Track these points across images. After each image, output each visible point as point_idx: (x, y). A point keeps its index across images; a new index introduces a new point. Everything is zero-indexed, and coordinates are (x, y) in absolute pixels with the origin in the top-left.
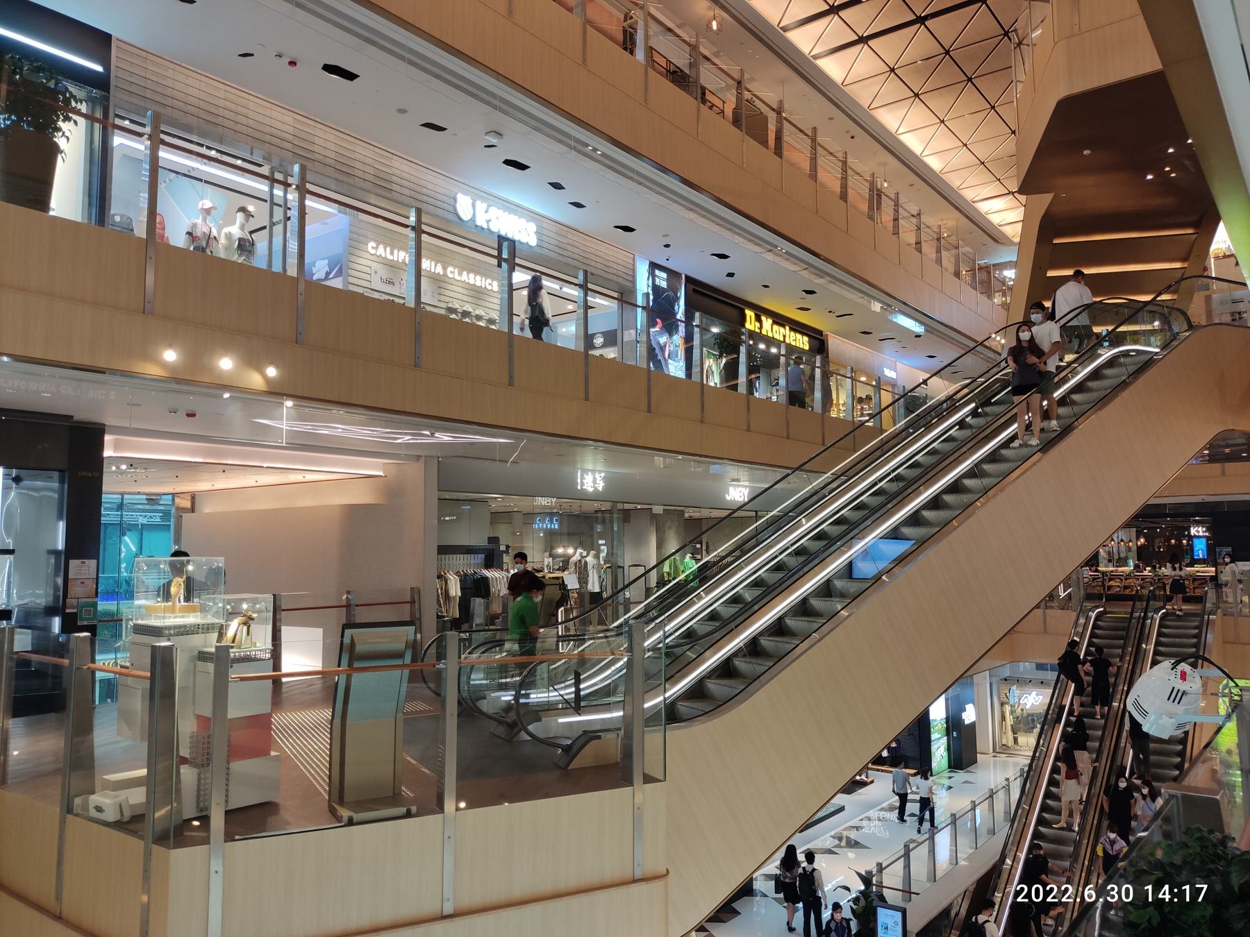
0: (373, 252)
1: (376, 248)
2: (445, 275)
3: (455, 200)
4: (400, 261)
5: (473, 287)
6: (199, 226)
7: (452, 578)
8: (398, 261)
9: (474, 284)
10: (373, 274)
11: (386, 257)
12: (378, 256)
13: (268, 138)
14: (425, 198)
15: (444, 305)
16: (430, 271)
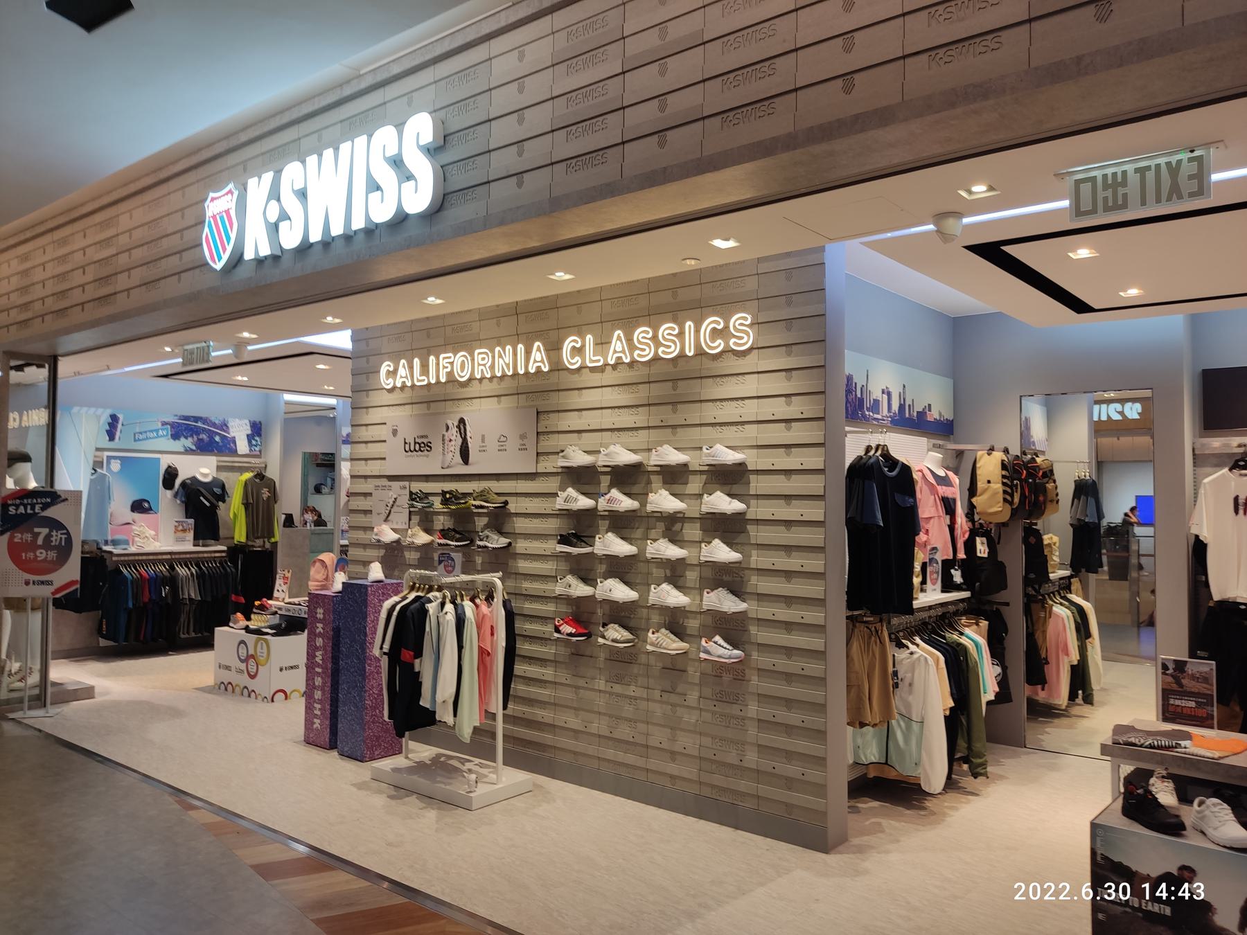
2: (558, 367)
4: (443, 380)
5: (655, 369)
8: (438, 382)
9: (656, 359)
15: (548, 465)
16: (515, 374)
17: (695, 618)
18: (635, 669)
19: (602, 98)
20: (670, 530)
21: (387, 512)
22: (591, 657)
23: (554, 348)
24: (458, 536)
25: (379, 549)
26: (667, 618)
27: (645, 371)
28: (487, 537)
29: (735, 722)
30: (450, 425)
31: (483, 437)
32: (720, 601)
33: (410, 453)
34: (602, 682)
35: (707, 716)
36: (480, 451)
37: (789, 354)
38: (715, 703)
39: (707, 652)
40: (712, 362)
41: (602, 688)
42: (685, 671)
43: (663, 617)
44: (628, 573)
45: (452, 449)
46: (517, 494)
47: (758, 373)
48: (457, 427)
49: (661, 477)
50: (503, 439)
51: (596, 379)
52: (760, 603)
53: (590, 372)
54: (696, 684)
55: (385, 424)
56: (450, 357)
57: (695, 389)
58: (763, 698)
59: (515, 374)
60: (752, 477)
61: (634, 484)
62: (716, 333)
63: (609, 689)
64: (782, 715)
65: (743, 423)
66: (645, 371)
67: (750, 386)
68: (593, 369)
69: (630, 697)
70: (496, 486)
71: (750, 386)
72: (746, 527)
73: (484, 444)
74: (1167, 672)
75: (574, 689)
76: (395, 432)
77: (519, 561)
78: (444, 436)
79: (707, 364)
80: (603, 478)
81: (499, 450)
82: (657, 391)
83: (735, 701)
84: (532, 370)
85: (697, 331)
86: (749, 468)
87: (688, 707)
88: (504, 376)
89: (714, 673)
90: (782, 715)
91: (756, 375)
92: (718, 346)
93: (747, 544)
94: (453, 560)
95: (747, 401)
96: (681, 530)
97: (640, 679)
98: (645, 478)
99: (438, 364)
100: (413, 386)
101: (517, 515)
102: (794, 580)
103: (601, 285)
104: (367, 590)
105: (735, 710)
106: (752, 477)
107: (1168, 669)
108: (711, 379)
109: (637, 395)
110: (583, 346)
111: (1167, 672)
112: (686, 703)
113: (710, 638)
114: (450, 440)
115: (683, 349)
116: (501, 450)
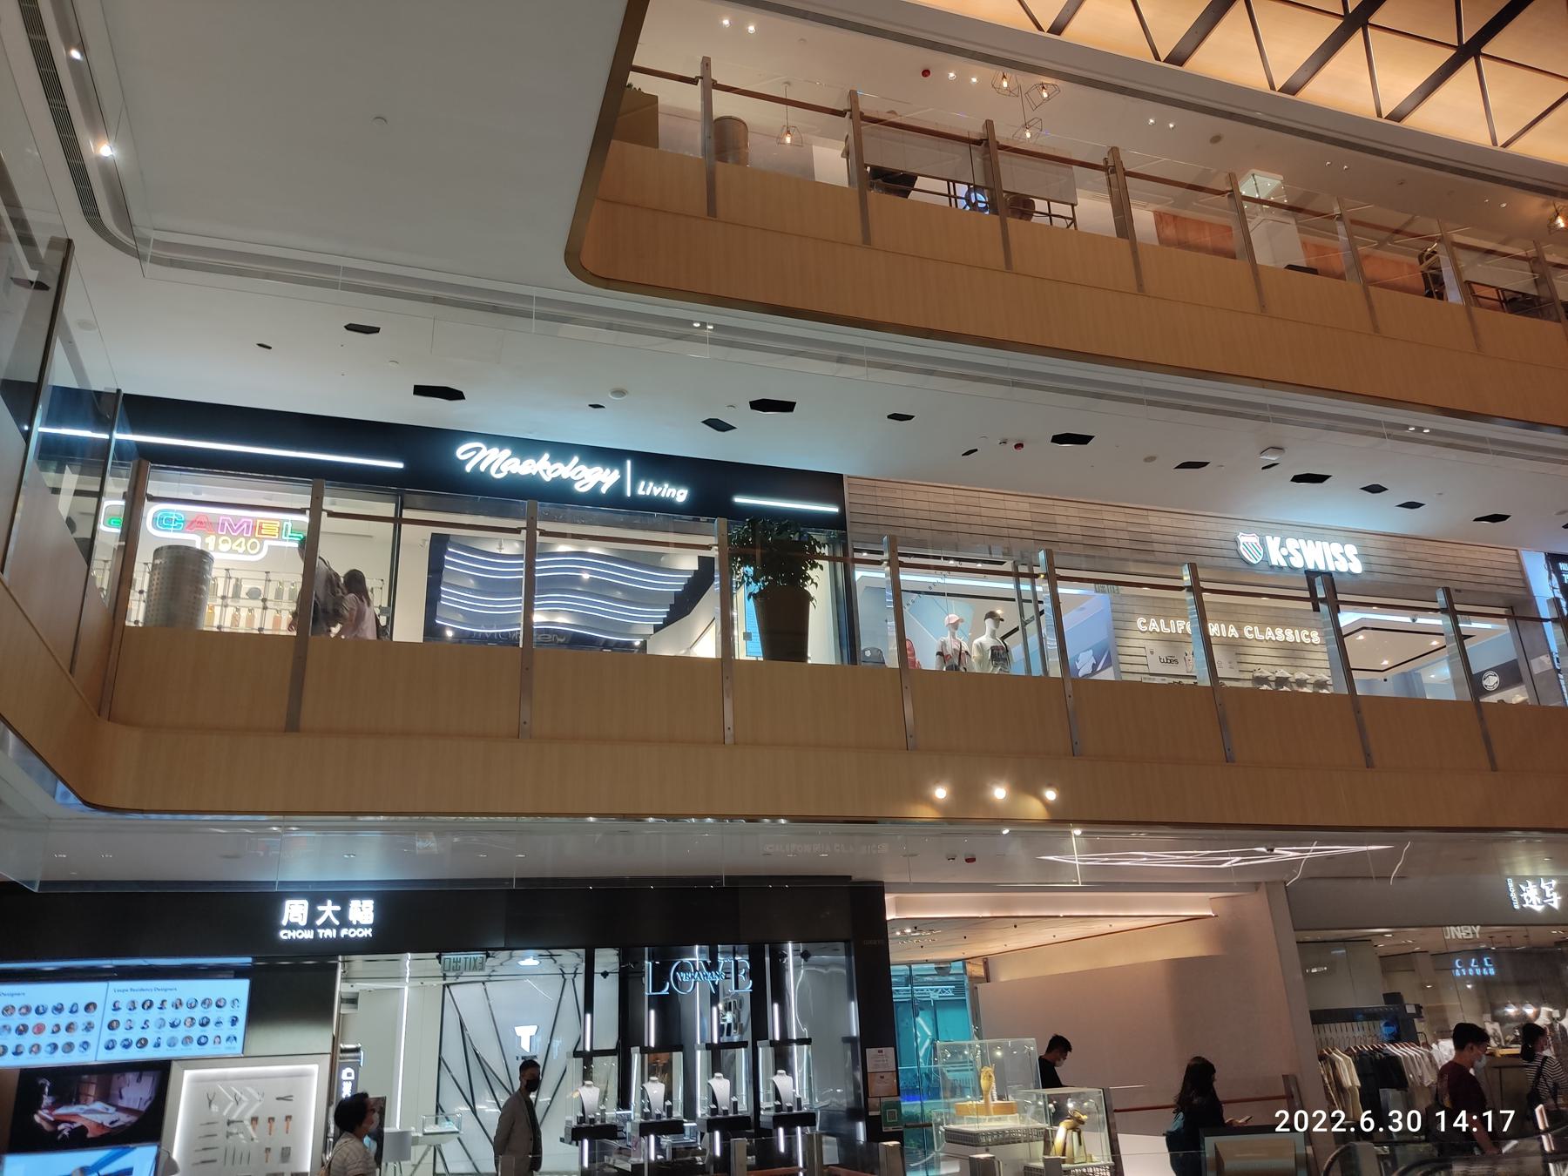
1: (1147, 624)
2: (1242, 637)
3: (1236, 542)
6: (949, 644)
7: (1339, 1058)
8: (1177, 633)
9: (1285, 641)
10: (1149, 655)
11: (1161, 632)
12: (1151, 632)
13: (1005, 532)
14: (1197, 550)
15: (1249, 676)
16: (1221, 636)
51: (1260, 644)
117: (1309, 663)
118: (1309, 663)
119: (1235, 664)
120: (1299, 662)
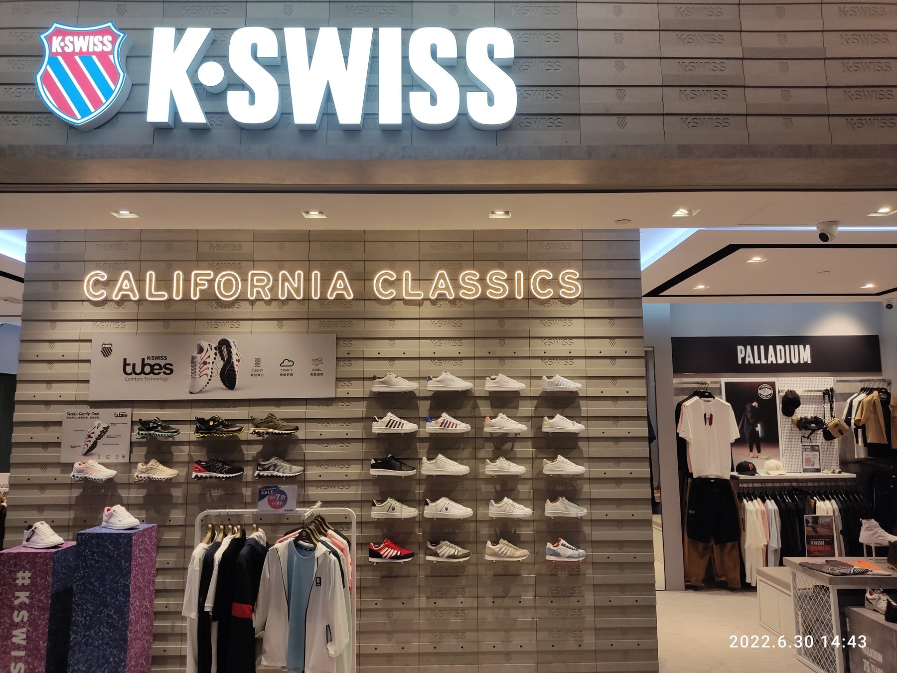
0: (102, 294)
1: (109, 284)
2: (365, 296)
8: (186, 299)
9: (483, 298)
15: (356, 390)
16: (307, 299)
17: (528, 526)
18: (463, 581)
19: (720, 73)
20: (501, 449)
21: (90, 444)
22: (408, 576)
23: (361, 278)
24: (227, 467)
25: (71, 489)
26: (497, 529)
27: (470, 308)
28: (275, 466)
29: (572, 613)
30: (205, 345)
31: (258, 362)
32: (566, 508)
33: (133, 376)
34: (423, 600)
35: (544, 613)
36: (281, 375)
37: (611, 306)
38: (552, 599)
39: (557, 554)
40: (540, 306)
41: (423, 605)
42: (518, 575)
43: (493, 529)
44: (453, 491)
45: (209, 372)
46: (306, 420)
47: (584, 318)
48: (215, 348)
49: (489, 401)
50: (286, 363)
51: (413, 311)
52: (592, 507)
53: (432, 304)
54: (531, 585)
55: (90, 341)
56: (209, 275)
57: (522, 327)
58: (598, 587)
59: (307, 299)
60: (582, 403)
61: (460, 408)
62: (544, 283)
63: (432, 605)
64: (618, 599)
65: (461, 359)
66: (470, 308)
67: (577, 328)
68: (407, 302)
69: (457, 609)
70: (281, 412)
71: (577, 328)
72: (578, 444)
73: (258, 368)
74: (809, 525)
75: (386, 613)
76: (107, 352)
77: (309, 488)
78: (193, 358)
79: (536, 308)
80: (421, 403)
81: (281, 375)
82: (480, 326)
83: (571, 594)
84: (331, 296)
85: (527, 279)
86: (580, 395)
87: (523, 608)
88: (290, 299)
89: (549, 572)
90: (618, 599)
91: (582, 320)
92: (548, 293)
93: (578, 458)
94: (283, 493)
95: (574, 341)
96: (512, 449)
97: (467, 590)
98: (471, 403)
99: (187, 280)
100: (142, 301)
101: (306, 441)
102: (623, 485)
103: (310, 229)
104: (131, 539)
105: (573, 602)
106: (582, 403)
107: (809, 523)
108: (539, 320)
109: (461, 329)
110: (399, 280)
111: (809, 525)
112: (521, 604)
113: (555, 542)
114: (205, 363)
115: (512, 291)
116: (285, 375)
117: (539, 348)
118: (539, 348)
119: (329, 368)
120: (508, 348)
